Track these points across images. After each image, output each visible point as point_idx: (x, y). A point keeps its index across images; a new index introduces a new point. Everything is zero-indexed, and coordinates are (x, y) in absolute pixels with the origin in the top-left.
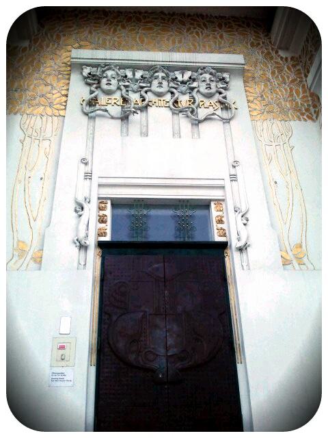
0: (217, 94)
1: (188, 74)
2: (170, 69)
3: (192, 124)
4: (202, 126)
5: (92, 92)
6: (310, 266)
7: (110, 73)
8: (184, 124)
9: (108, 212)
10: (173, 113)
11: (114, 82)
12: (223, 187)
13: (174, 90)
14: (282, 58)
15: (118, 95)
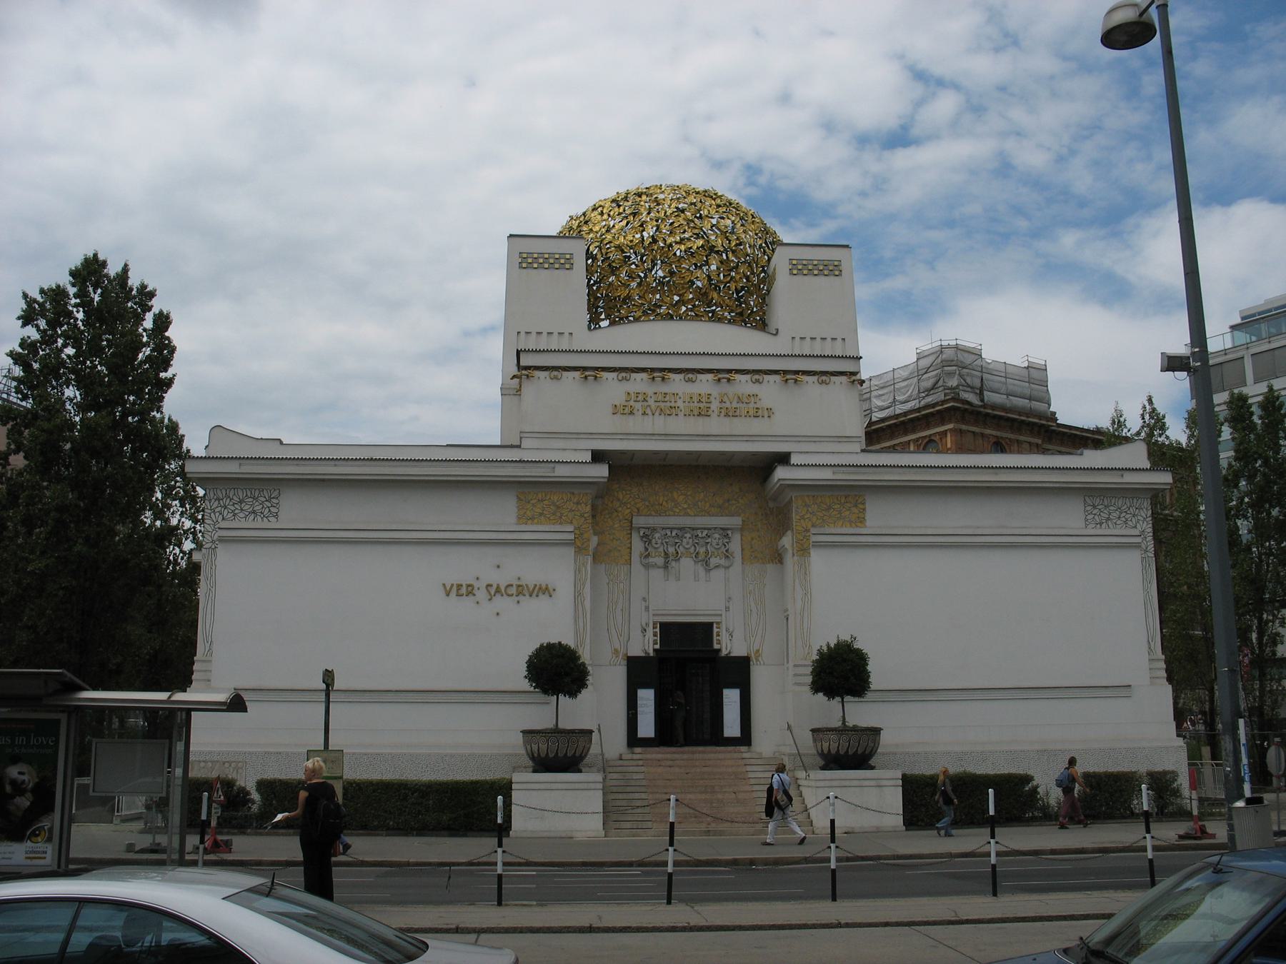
0: (723, 547)
1: (705, 532)
2: (693, 529)
3: (706, 569)
4: (713, 573)
5: (646, 549)
6: (762, 662)
7: (657, 535)
8: (701, 570)
9: (658, 630)
10: (695, 561)
11: (659, 541)
12: (721, 615)
13: (696, 545)
14: (770, 508)
15: (661, 549)
